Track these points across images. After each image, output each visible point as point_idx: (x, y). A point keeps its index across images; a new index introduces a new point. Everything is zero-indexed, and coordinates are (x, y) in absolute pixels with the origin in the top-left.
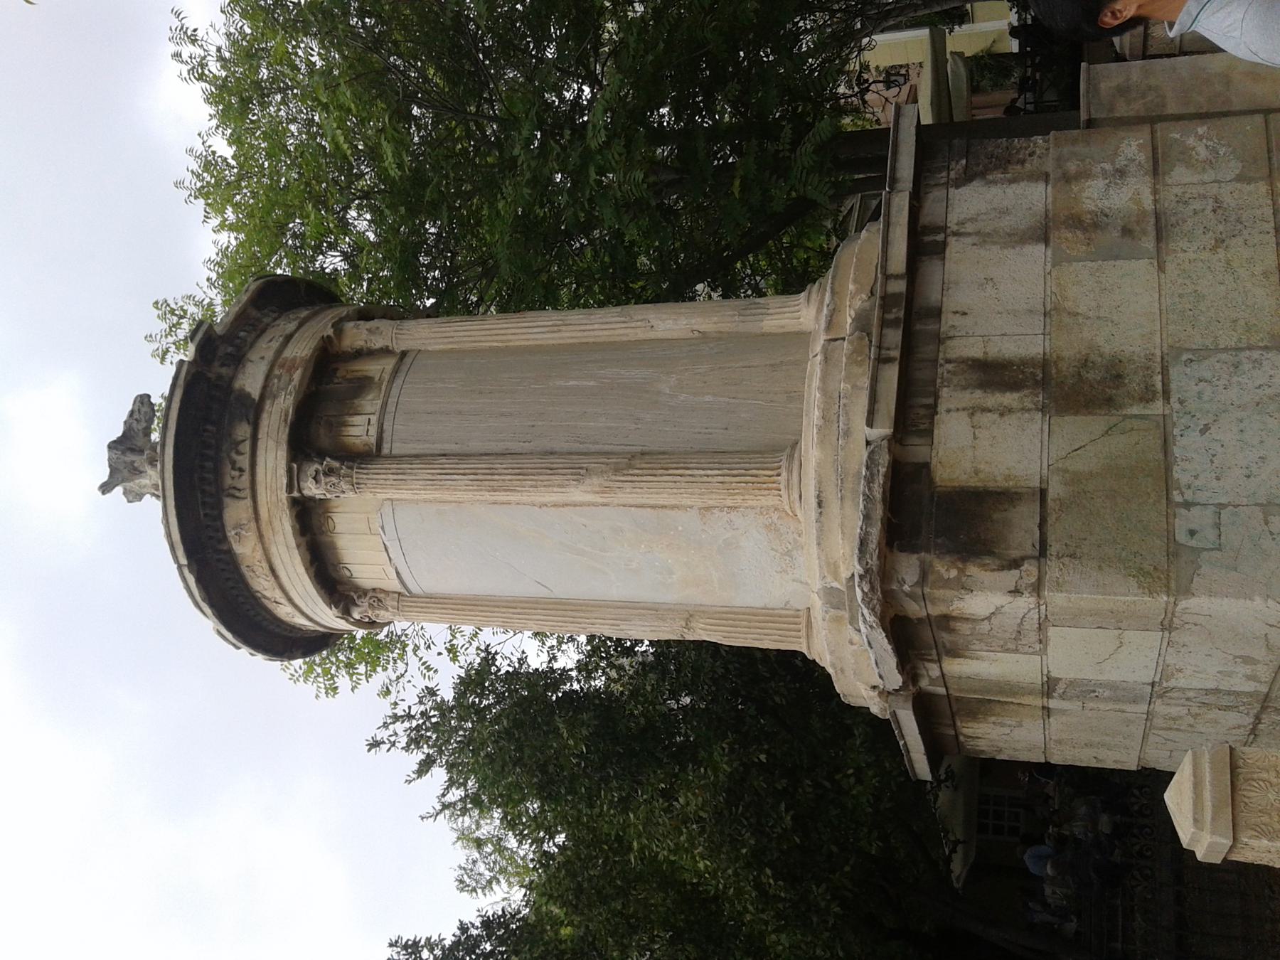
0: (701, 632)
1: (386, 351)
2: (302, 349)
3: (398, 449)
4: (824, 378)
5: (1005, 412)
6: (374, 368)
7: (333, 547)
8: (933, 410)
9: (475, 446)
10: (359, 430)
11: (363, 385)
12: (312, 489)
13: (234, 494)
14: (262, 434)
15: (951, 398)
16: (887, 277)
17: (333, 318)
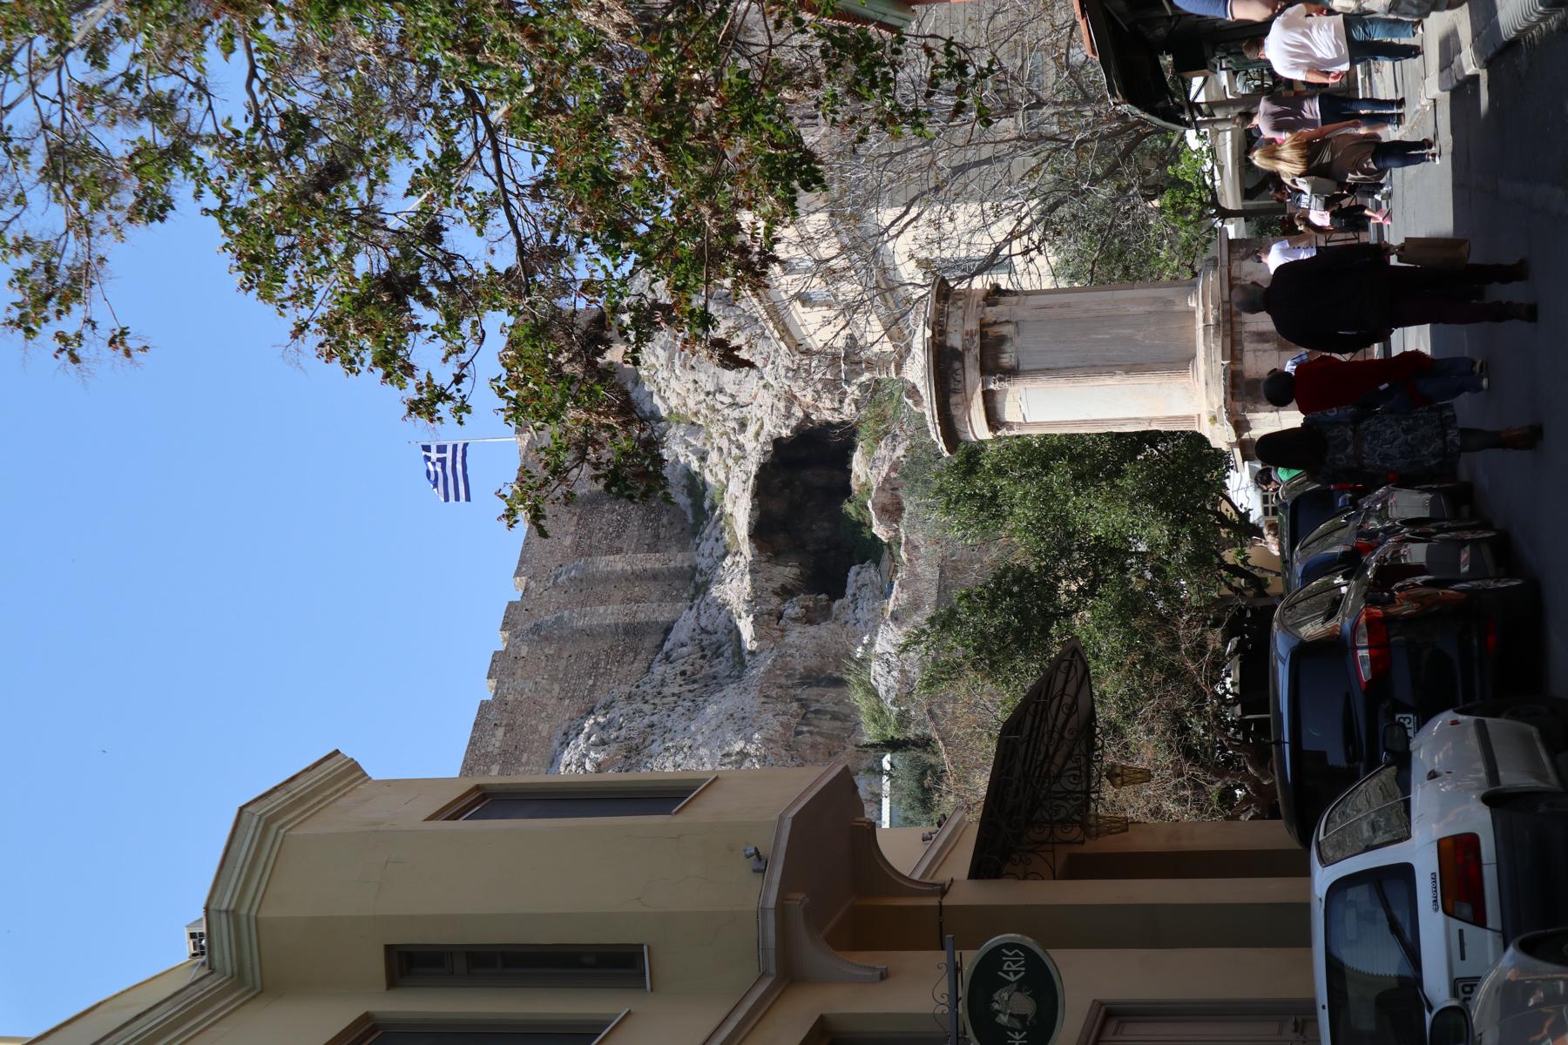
0: (1154, 427)
1: (1008, 322)
2: (973, 326)
3: (1026, 367)
4: (1205, 340)
5: (1265, 351)
6: (1006, 330)
7: (994, 408)
8: (1242, 350)
9: (1061, 365)
10: (1007, 360)
11: (1002, 340)
12: (992, 386)
13: (955, 392)
14: (967, 365)
15: (1248, 346)
16: (1223, 302)
17: (978, 306)
